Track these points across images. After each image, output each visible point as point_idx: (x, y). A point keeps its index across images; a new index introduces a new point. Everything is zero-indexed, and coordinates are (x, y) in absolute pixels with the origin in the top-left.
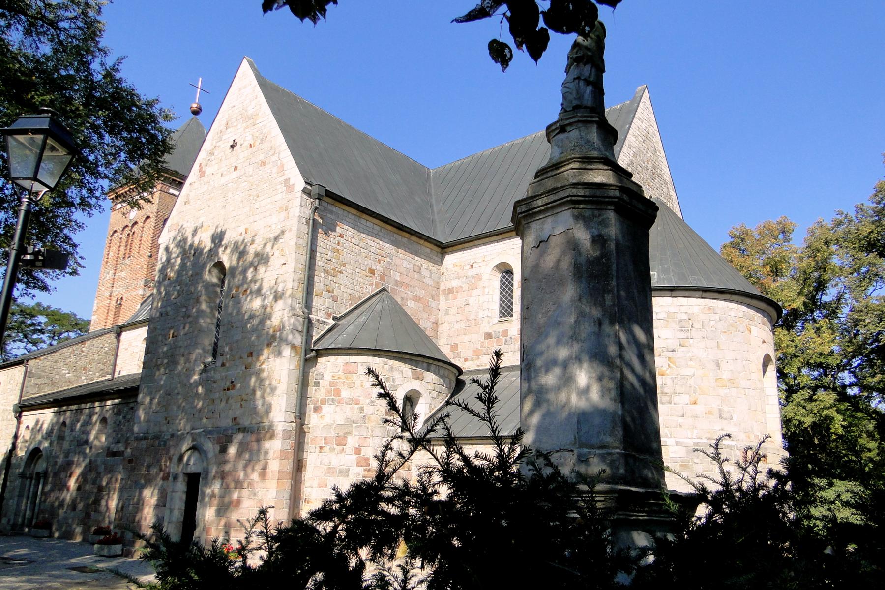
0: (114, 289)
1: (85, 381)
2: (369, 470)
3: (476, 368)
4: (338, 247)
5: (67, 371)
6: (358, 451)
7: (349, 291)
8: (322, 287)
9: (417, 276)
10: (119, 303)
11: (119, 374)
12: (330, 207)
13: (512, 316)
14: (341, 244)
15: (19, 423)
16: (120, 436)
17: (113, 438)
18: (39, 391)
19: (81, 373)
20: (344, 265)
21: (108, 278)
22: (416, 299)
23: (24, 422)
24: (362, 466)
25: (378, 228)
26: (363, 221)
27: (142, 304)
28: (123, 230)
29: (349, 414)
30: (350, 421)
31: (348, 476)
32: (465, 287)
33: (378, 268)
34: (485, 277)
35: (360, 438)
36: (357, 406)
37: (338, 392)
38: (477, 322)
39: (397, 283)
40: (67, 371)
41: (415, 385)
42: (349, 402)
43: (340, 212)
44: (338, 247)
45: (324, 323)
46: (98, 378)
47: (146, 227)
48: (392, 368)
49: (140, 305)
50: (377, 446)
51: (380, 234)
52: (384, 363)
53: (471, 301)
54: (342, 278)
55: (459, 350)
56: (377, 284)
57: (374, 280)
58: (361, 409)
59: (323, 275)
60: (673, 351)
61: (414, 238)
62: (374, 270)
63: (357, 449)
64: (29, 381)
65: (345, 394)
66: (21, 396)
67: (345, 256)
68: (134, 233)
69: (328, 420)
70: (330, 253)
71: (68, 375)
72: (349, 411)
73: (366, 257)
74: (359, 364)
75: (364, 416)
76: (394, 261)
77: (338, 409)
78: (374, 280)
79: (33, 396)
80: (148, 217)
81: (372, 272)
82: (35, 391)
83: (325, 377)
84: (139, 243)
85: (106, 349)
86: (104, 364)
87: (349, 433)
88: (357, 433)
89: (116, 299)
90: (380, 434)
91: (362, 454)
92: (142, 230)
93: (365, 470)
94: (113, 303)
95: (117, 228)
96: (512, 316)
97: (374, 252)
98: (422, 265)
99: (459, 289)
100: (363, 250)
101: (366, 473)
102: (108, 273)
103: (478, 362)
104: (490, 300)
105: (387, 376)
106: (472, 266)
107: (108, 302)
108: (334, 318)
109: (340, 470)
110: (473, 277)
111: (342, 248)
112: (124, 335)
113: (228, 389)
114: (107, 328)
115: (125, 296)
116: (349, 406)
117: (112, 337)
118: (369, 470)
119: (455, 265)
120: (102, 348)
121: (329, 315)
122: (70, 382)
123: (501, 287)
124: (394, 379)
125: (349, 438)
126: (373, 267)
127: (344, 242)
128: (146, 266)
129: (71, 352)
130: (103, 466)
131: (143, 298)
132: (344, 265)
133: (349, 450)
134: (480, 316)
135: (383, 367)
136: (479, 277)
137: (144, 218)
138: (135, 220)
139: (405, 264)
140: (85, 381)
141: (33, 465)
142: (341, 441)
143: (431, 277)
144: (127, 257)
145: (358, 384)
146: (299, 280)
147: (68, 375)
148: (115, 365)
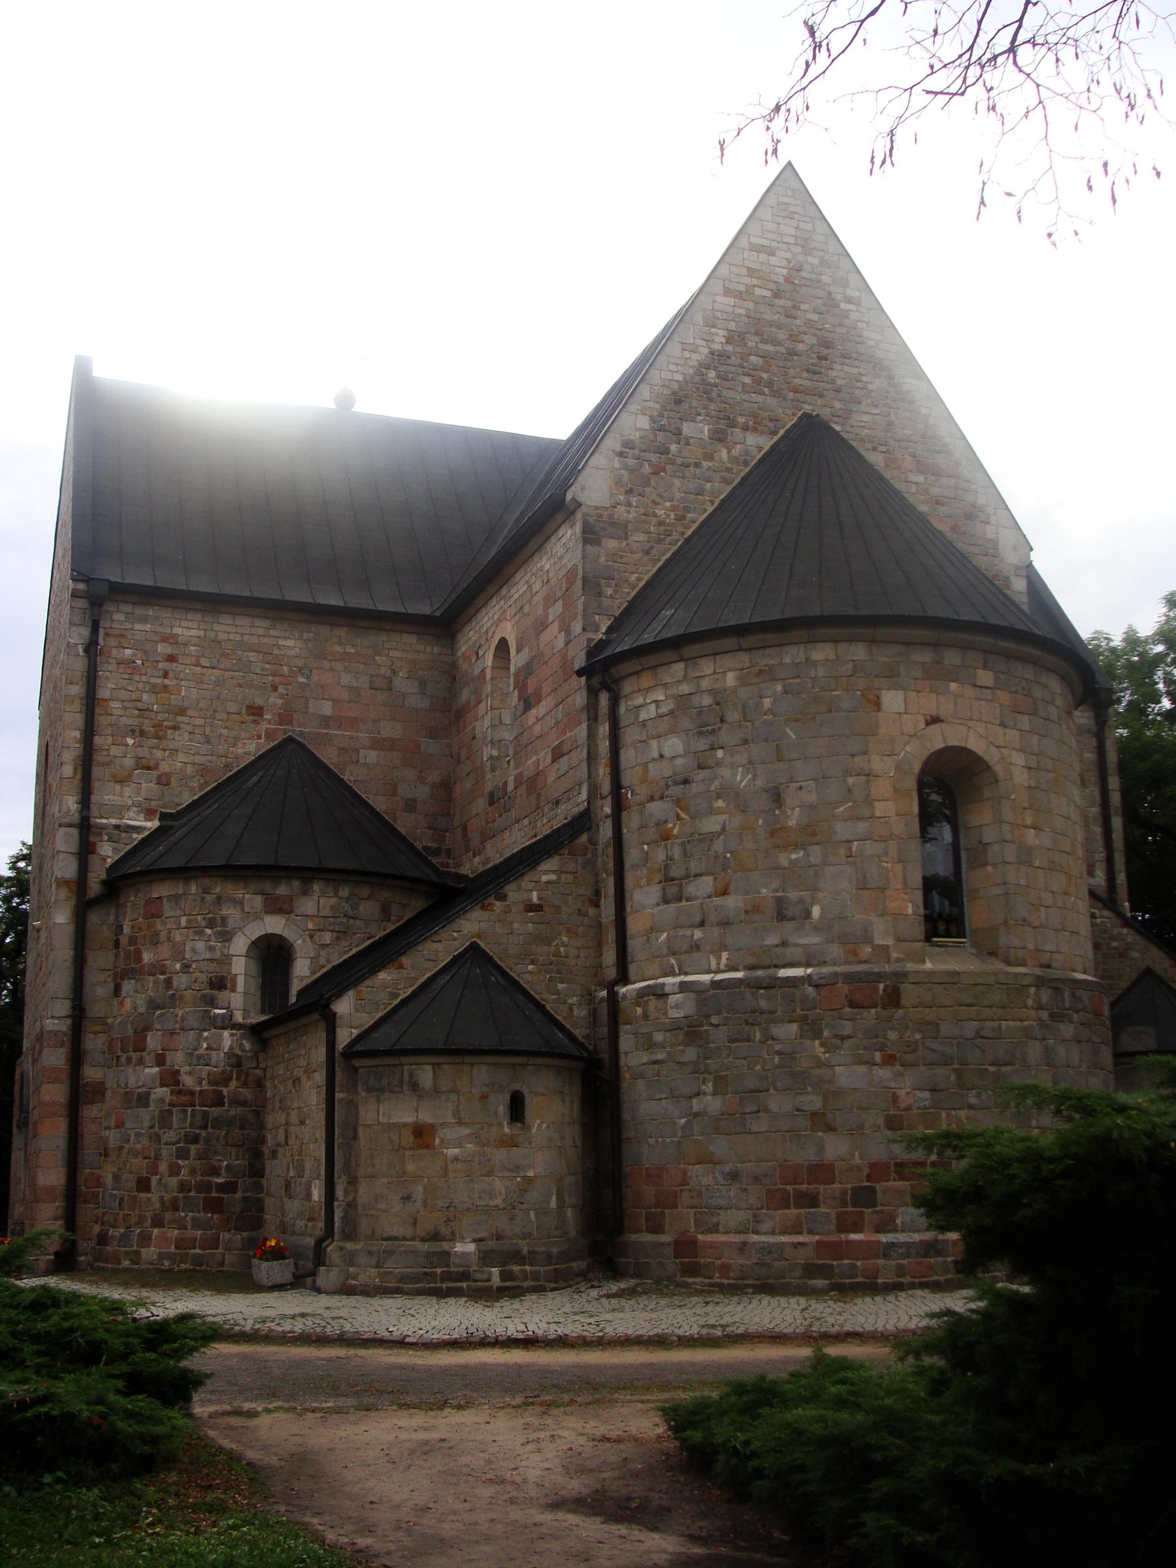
2: (180, 1092)
4: (167, 681)
6: (160, 1060)
7: (199, 759)
8: (129, 762)
9: (381, 697)
12: (139, 611)
14: (171, 674)
20: (182, 711)
24: (167, 1086)
31: (147, 1105)
35: (163, 1035)
36: (162, 977)
39: (326, 721)
41: (274, 925)
43: (166, 614)
44: (167, 681)
48: (219, 898)
50: (191, 1047)
51: (272, 632)
52: (206, 891)
56: (270, 735)
57: (264, 726)
58: (168, 983)
59: (130, 741)
62: (261, 708)
63: (160, 1054)
65: (147, 957)
67: (187, 692)
70: (145, 697)
73: (240, 685)
74: (165, 900)
75: (173, 995)
76: (315, 678)
78: (264, 726)
81: (256, 712)
87: (148, 1028)
88: (159, 1027)
90: (196, 1025)
91: (168, 1062)
93: (172, 1093)
97: (258, 671)
98: (394, 672)
100: (228, 674)
101: (174, 1098)
104: (497, 723)
105: (210, 916)
109: (138, 1095)
111: (175, 682)
116: (151, 978)
118: (180, 1092)
124: (224, 920)
125: (153, 1041)
126: (259, 702)
127: (181, 667)
133: (149, 1058)
135: (203, 899)
139: (346, 679)
142: (140, 1047)
143: (423, 692)
145: (163, 936)
146: (73, 760)
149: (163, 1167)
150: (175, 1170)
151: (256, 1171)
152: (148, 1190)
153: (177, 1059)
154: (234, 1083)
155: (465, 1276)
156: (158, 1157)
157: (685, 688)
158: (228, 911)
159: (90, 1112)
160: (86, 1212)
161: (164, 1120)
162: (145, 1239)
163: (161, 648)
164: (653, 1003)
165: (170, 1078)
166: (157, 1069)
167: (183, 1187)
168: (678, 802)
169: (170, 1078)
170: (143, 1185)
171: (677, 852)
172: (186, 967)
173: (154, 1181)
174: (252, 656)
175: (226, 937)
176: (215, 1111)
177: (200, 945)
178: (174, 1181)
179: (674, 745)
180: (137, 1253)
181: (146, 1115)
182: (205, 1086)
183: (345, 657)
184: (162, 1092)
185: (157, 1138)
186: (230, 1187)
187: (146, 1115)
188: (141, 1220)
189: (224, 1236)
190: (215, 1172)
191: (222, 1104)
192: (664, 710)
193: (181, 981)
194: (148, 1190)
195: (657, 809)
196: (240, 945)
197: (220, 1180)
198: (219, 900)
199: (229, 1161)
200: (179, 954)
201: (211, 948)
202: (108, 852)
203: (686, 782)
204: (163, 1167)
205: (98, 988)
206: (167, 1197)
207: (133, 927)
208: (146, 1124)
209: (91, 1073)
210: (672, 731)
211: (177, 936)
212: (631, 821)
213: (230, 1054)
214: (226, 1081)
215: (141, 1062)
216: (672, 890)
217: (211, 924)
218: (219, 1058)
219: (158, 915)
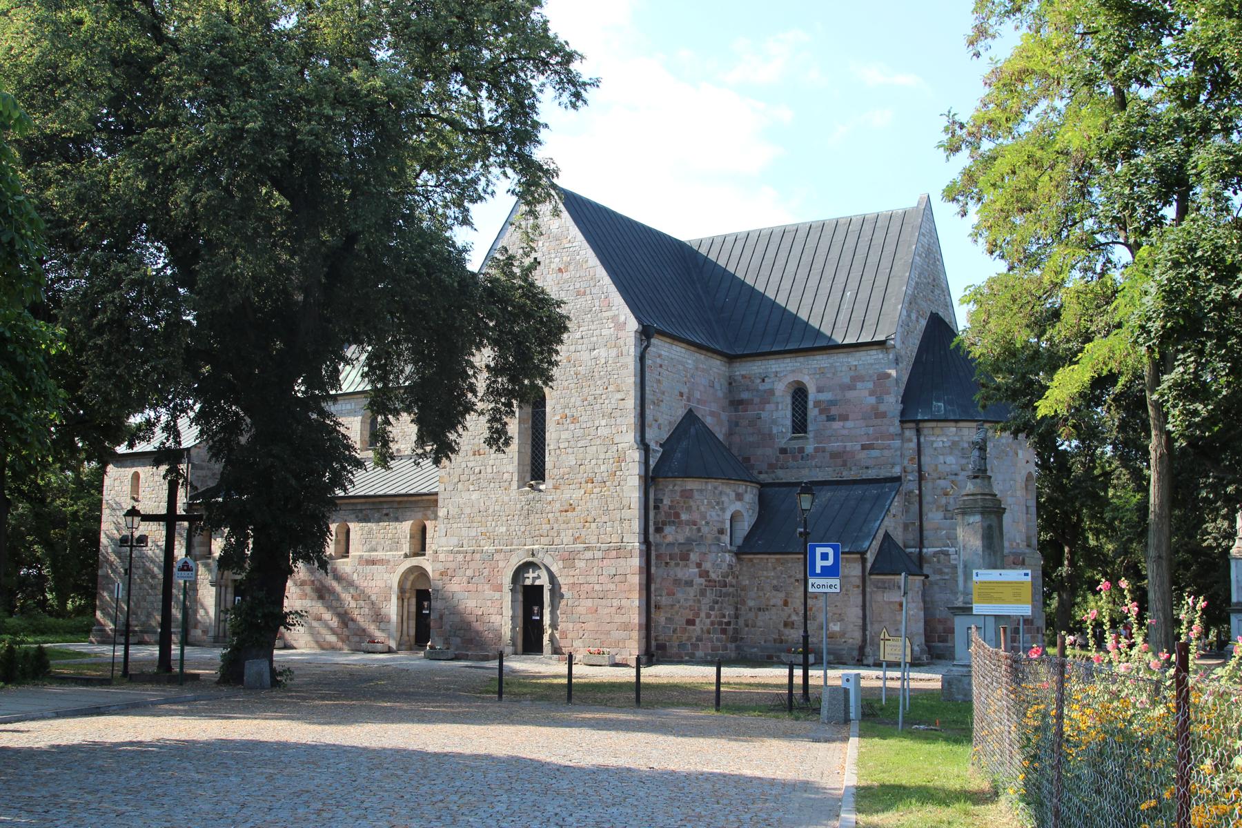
3: (771, 481)
6: (699, 565)
13: (806, 432)
22: (712, 414)
25: (683, 350)
26: (674, 347)
29: (688, 533)
30: (689, 541)
32: (757, 400)
33: (685, 390)
34: (777, 393)
37: (677, 515)
38: (771, 436)
41: (738, 506)
42: (688, 523)
45: (658, 451)
53: (764, 415)
54: (663, 406)
55: (752, 462)
56: (685, 405)
58: (699, 530)
60: (956, 474)
61: (709, 354)
65: (684, 517)
69: (670, 539)
72: (687, 532)
77: (679, 530)
81: (681, 394)
83: (665, 502)
96: (806, 432)
99: (750, 402)
103: (773, 476)
106: (763, 381)
108: (661, 445)
110: (765, 391)
113: (566, 511)
118: (710, 581)
119: (744, 377)
121: (657, 442)
123: (793, 403)
125: (692, 555)
132: (663, 393)
134: (775, 431)
136: (771, 392)
142: (685, 557)
145: (694, 508)
149: (703, 615)
150: (708, 616)
151: (737, 617)
152: (694, 625)
153: (707, 566)
154: (730, 577)
155: (919, 659)
156: (699, 609)
157: (956, 439)
158: (724, 499)
159: (653, 587)
160: (653, 634)
161: (703, 593)
162: (695, 646)
163: (659, 361)
164: (942, 557)
165: (704, 574)
166: (697, 570)
167: (712, 623)
168: (952, 482)
169: (704, 574)
170: (691, 622)
171: (952, 501)
172: (707, 523)
173: (697, 621)
174: (681, 368)
175: (723, 510)
176: (724, 590)
177: (714, 514)
178: (708, 621)
179: (951, 459)
180: (694, 654)
181: (692, 592)
182: (720, 578)
183: (703, 370)
184: (702, 581)
185: (699, 601)
186: (728, 624)
187: (692, 592)
188: (689, 638)
189: (729, 645)
190: (724, 616)
191: (726, 586)
192: (946, 445)
193: (705, 530)
194: (694, 625)
195: (942, 483)
196: (728, 516)
197: (725, 620)
198: (721, 493)
199: (729, 611)
200: (704, 517)
201: (718, 515)
202: (652, 463)
203: (956, 474)
204: (703, 615)
205: (651, 529)
206: (705, 628)
207: (672, 501)
208: (692, 594)
209: (653, 570)
210: (951, 454)
211: (703, 509)
212: (927, 486)
213: (729, 565)
214: (728, 577)
215: (686, 566)
216: (949, 515)
217: (718, 504)
218: (725, 567)
219: (691, 497)
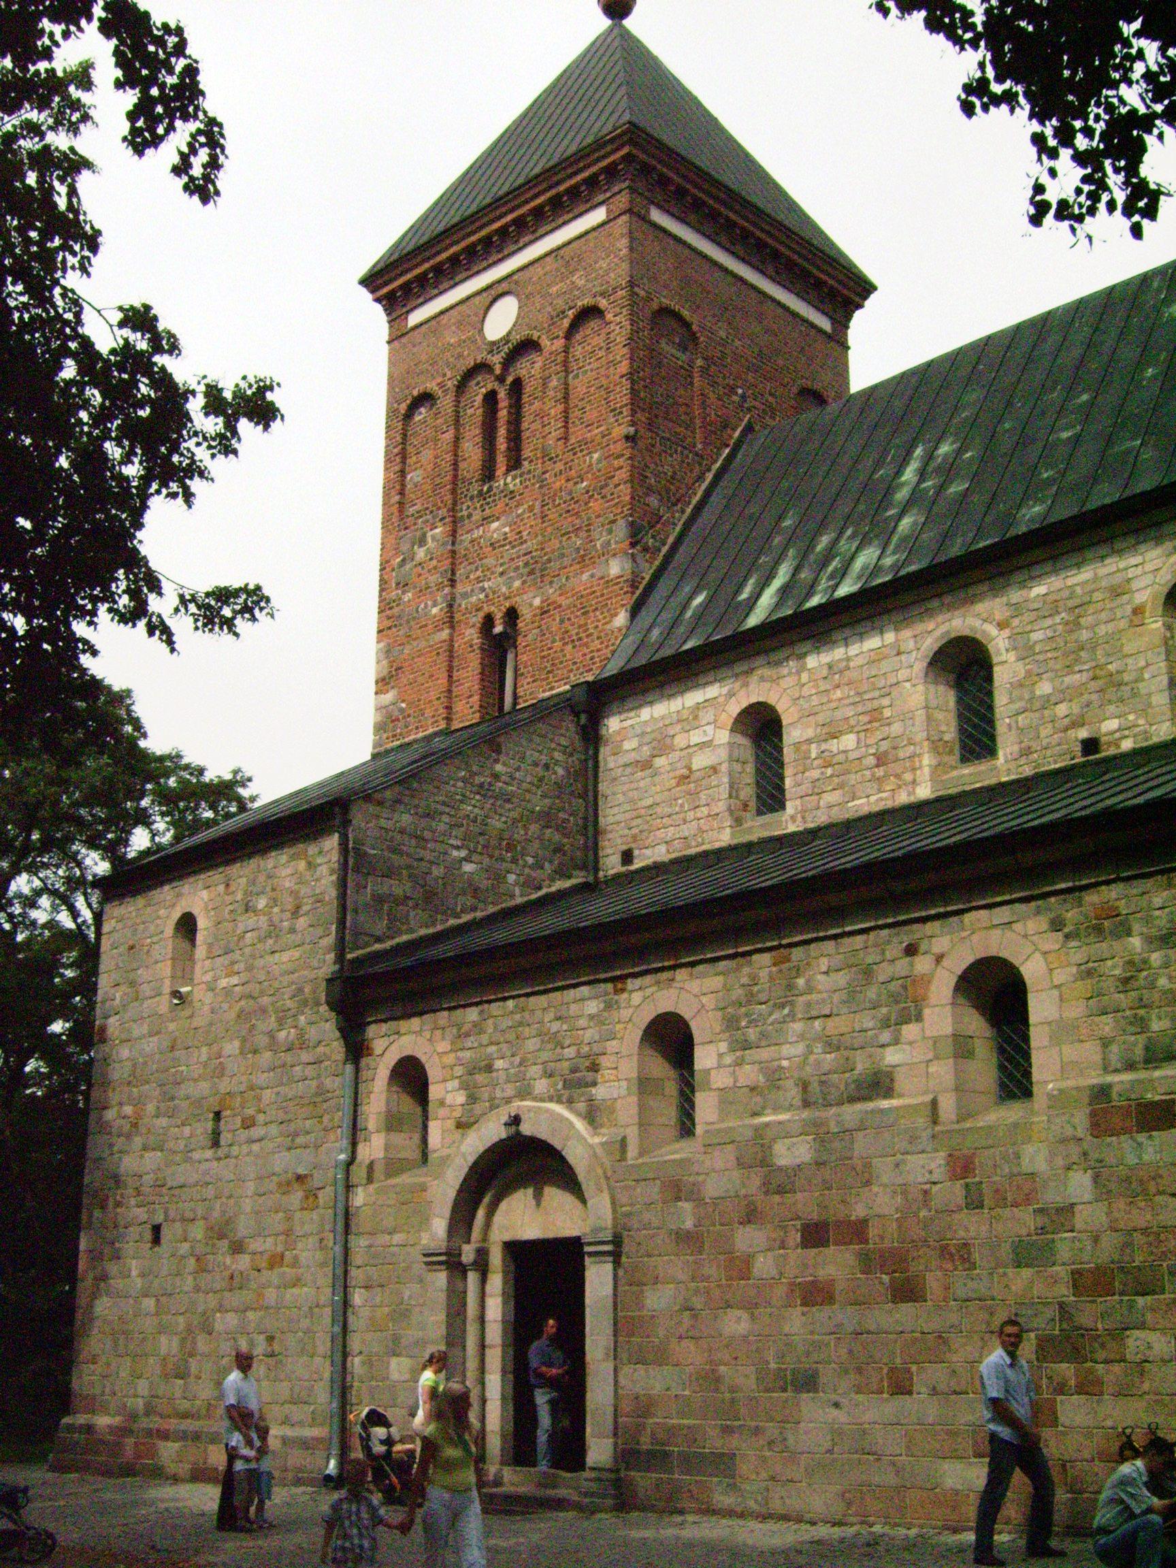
0: (460, 588)
1: (517, 891)
5: (463, 853)
10: (498, 629)
11: (627, 857)
15: (357, 1050)
16: (1156, 1026)
17: (1105, 1043)
18: (392, 932)
19: (503, 860)
21: (421, 553)
23: (378, 1046)
27: (635, 612)
28: (461, 387)
40: (463, 853)
46: (553, 880)
47: (578, 351)
49: (621, 619)
64: (360, 887)
66: (341, 948)
68: (517, 385)
71: (468, 868)
79: (377, 947)
80: (590, 313)
82: (381, 927)
84: (561, 407)
85: (560, 771)
86: (561, 828)
89: (478, 619)
92: (565, 363)
94: (471, 634)
95: (432, 386)
102: (422, 542)
107: (445, 634)
112: (613, 724)
114: (456, 725)
115: (530, 602)
117: (568, 732)
120: (547, 767)
122: (476, 891)
128: (623, 474)
129: (464, 780)
130: (1080, 1185)
131: (634, 585)
137: (566, 323)
138: (516, 338)
140: (517, 891)
141: (481, 1213)
144: (501, 469)
147: (468, 868)
148: (591, 831)
